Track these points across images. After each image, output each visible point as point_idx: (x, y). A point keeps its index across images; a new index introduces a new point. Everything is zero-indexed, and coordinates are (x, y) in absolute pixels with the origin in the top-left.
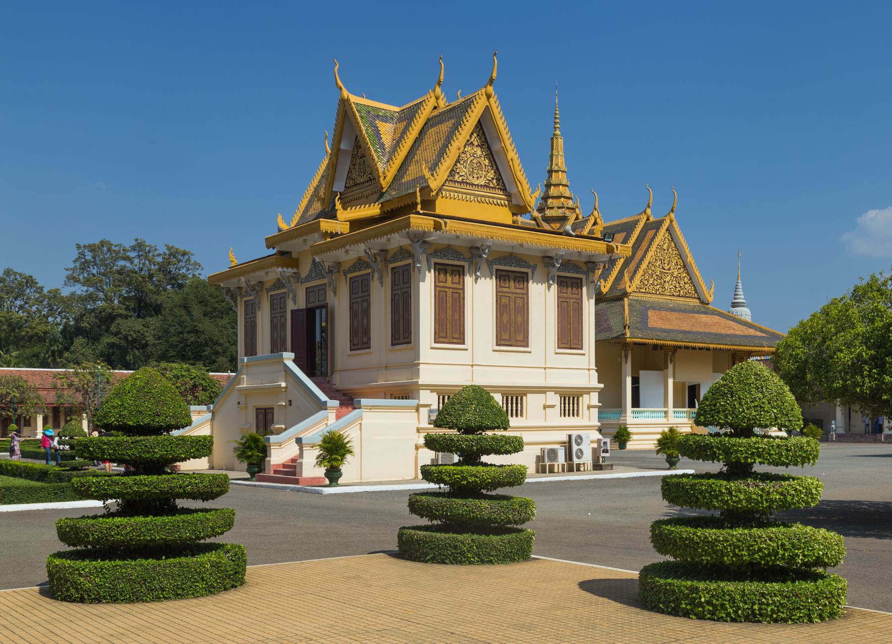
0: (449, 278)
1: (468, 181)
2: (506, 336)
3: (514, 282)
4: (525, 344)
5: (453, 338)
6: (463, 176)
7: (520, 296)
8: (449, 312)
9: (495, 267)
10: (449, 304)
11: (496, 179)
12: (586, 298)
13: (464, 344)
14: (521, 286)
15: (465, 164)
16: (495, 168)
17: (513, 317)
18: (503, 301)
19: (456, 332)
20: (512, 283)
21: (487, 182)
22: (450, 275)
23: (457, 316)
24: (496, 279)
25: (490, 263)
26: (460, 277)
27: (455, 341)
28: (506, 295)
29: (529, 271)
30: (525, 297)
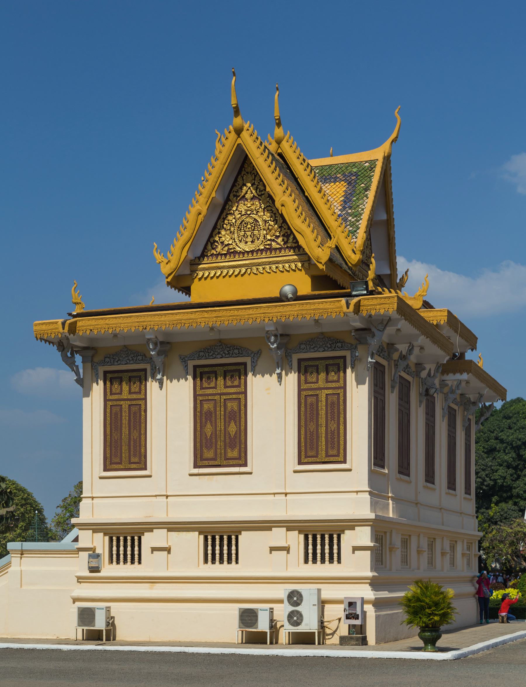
0: (125, 387)
1: (238, 249)
2: (208, 454)
3: (225, 379)
4: (241, 462)
5: (130, 463)
6: (230, 244)
7: (234, 396)
8: (125, 431)
9: (191, 364)
10: (125, 421)
11: (283, 236)
12: (354, 383)
13: (145, 469)
14: (236, 383)
15: (232, 229)
16: (280, 221)
17: (220, 425)
18: (206, 406)
19: (135, 456)
20: (220, 381)
21: (269, 242)
22: (127, 384)
23: (135, 435)
24: (194, 378)
25: (184, 360)
26: (141, 383)
27: (134, 466)
28: (210, 398)
29: (248, 360)
30: (242, 396)
